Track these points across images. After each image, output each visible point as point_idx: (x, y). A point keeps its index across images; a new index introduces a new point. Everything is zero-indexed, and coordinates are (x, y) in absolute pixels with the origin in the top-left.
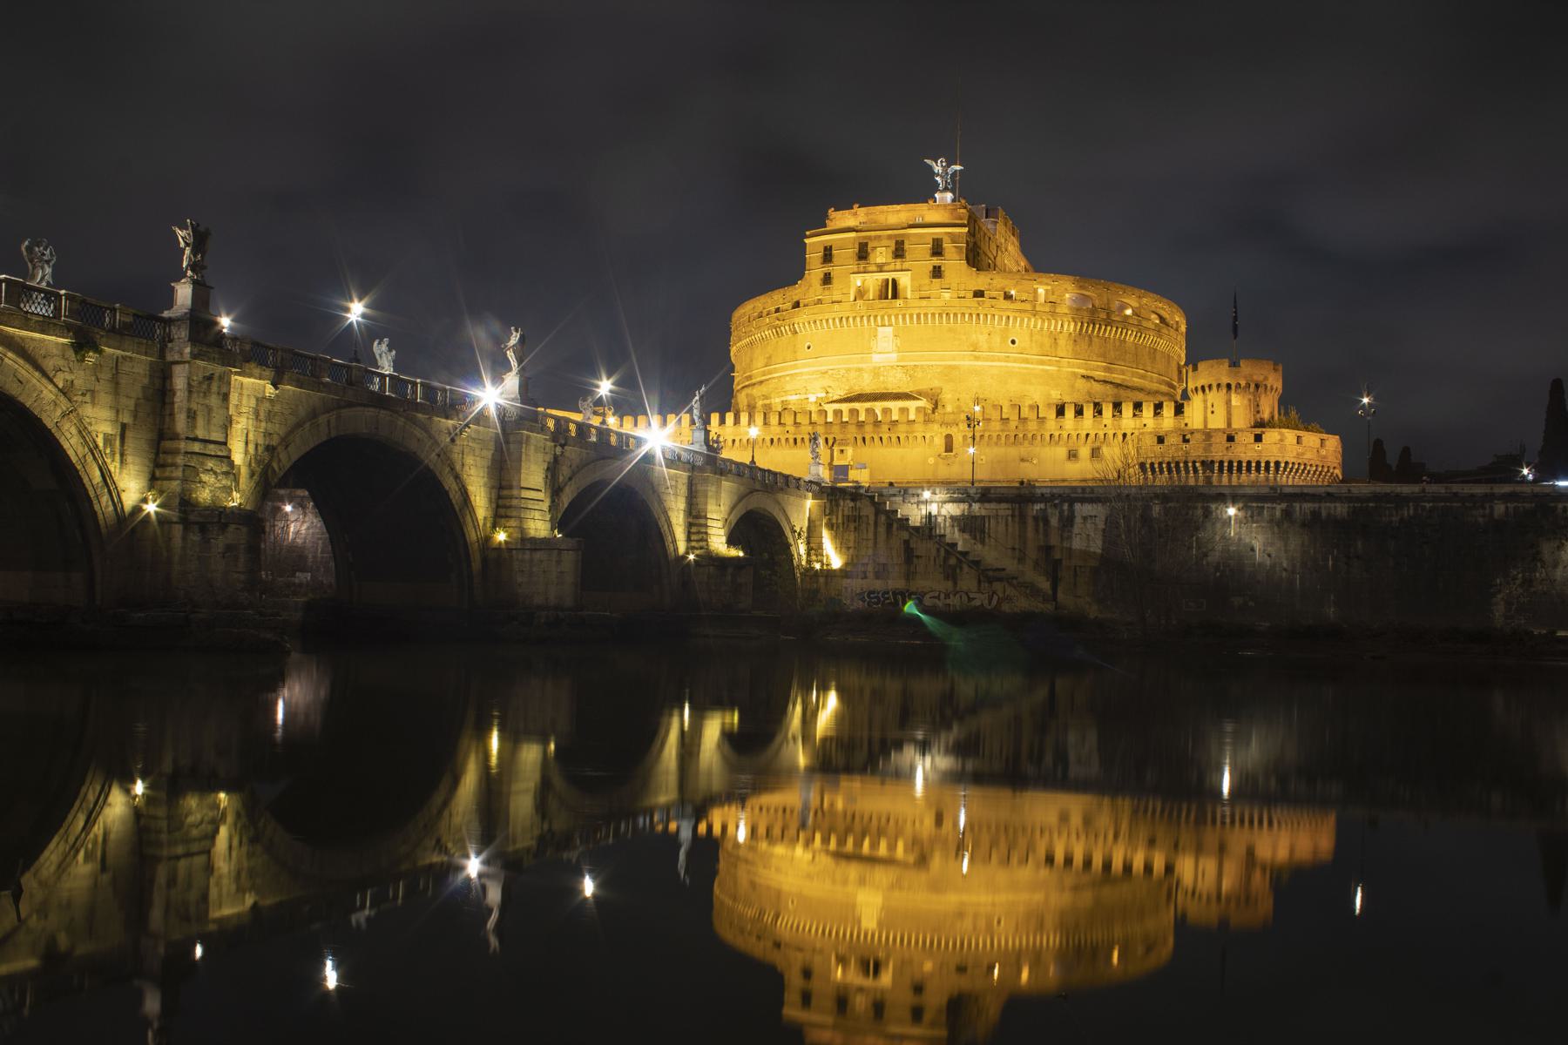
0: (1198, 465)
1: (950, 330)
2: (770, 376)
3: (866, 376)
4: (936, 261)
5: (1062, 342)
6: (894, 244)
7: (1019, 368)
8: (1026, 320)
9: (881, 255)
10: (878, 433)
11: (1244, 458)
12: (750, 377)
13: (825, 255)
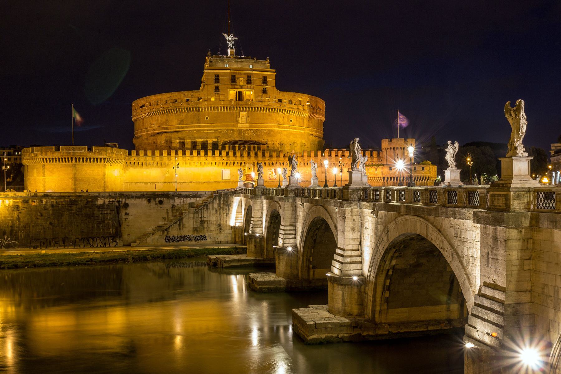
0: (405, 178)
1: (270, 115)
3: (235, 133)
4: (264, 86)
5: (305, 121)
6: (247, 77)
7: (293, 131)
8: (296, 112)
9: (241, 81)
10: (264, 161)
11: (419, 175)
12: (167, 128)
13: (215, 79)
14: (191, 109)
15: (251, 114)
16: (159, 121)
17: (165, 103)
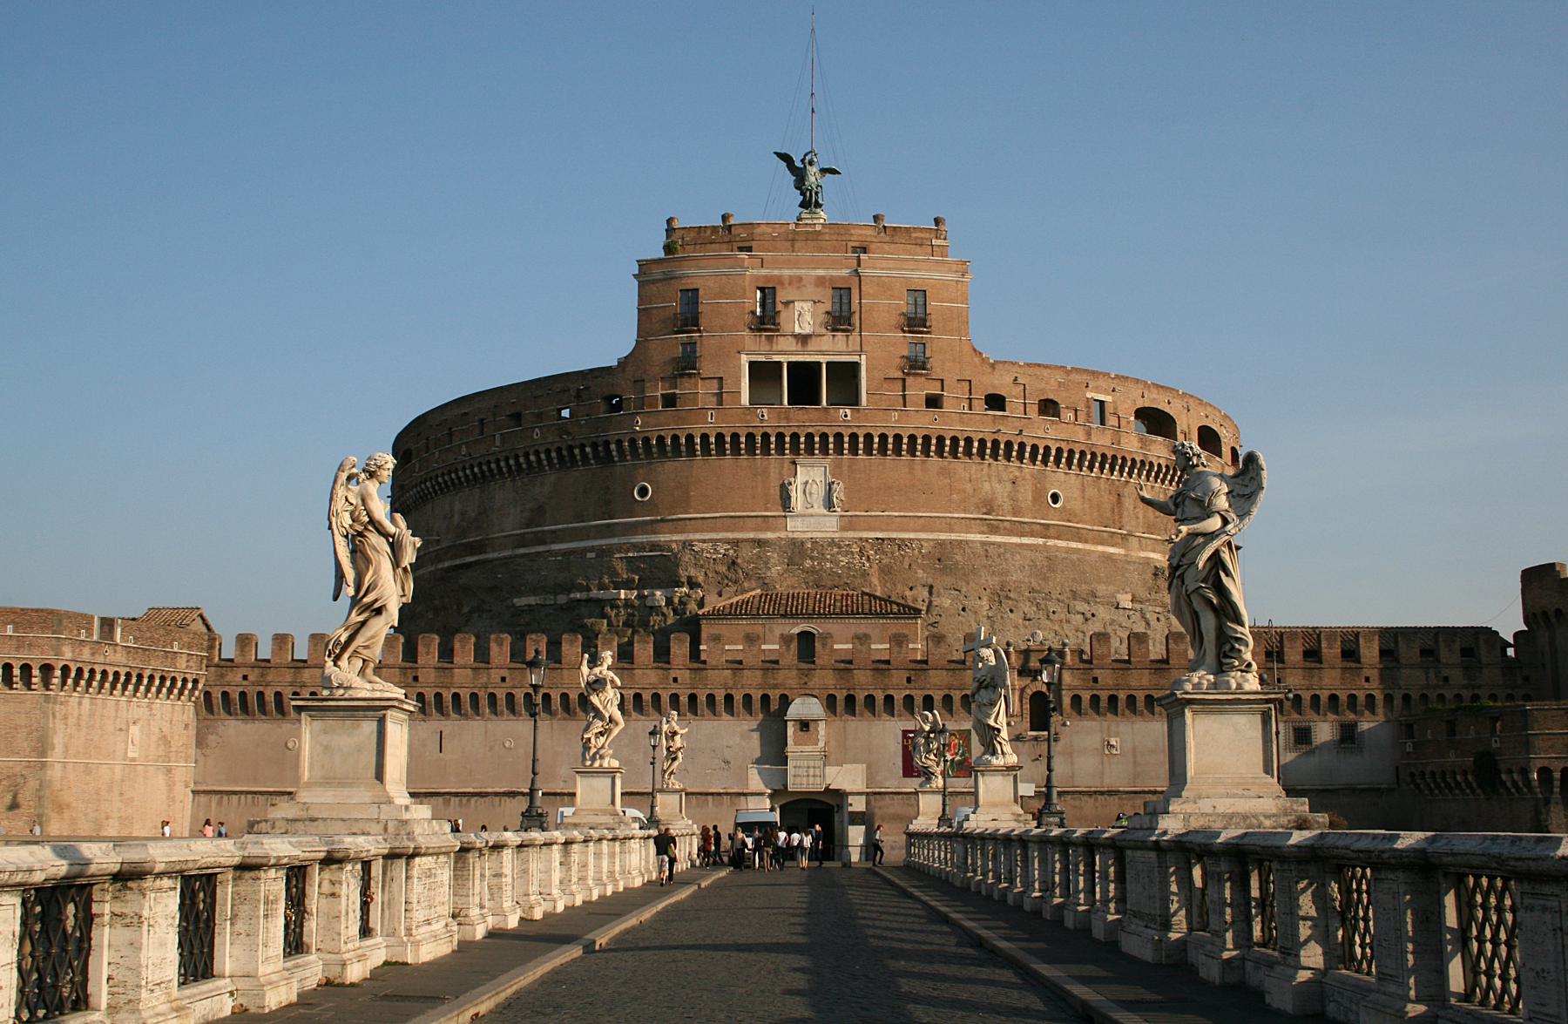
1: (943, 472)
2: (541, 549)
3: (774, 556)
7: (1069, 550)
9: (803, 316)
14: (577, 451)
15: (850, 467)
16: (456, 519)
17: (477, 431)
